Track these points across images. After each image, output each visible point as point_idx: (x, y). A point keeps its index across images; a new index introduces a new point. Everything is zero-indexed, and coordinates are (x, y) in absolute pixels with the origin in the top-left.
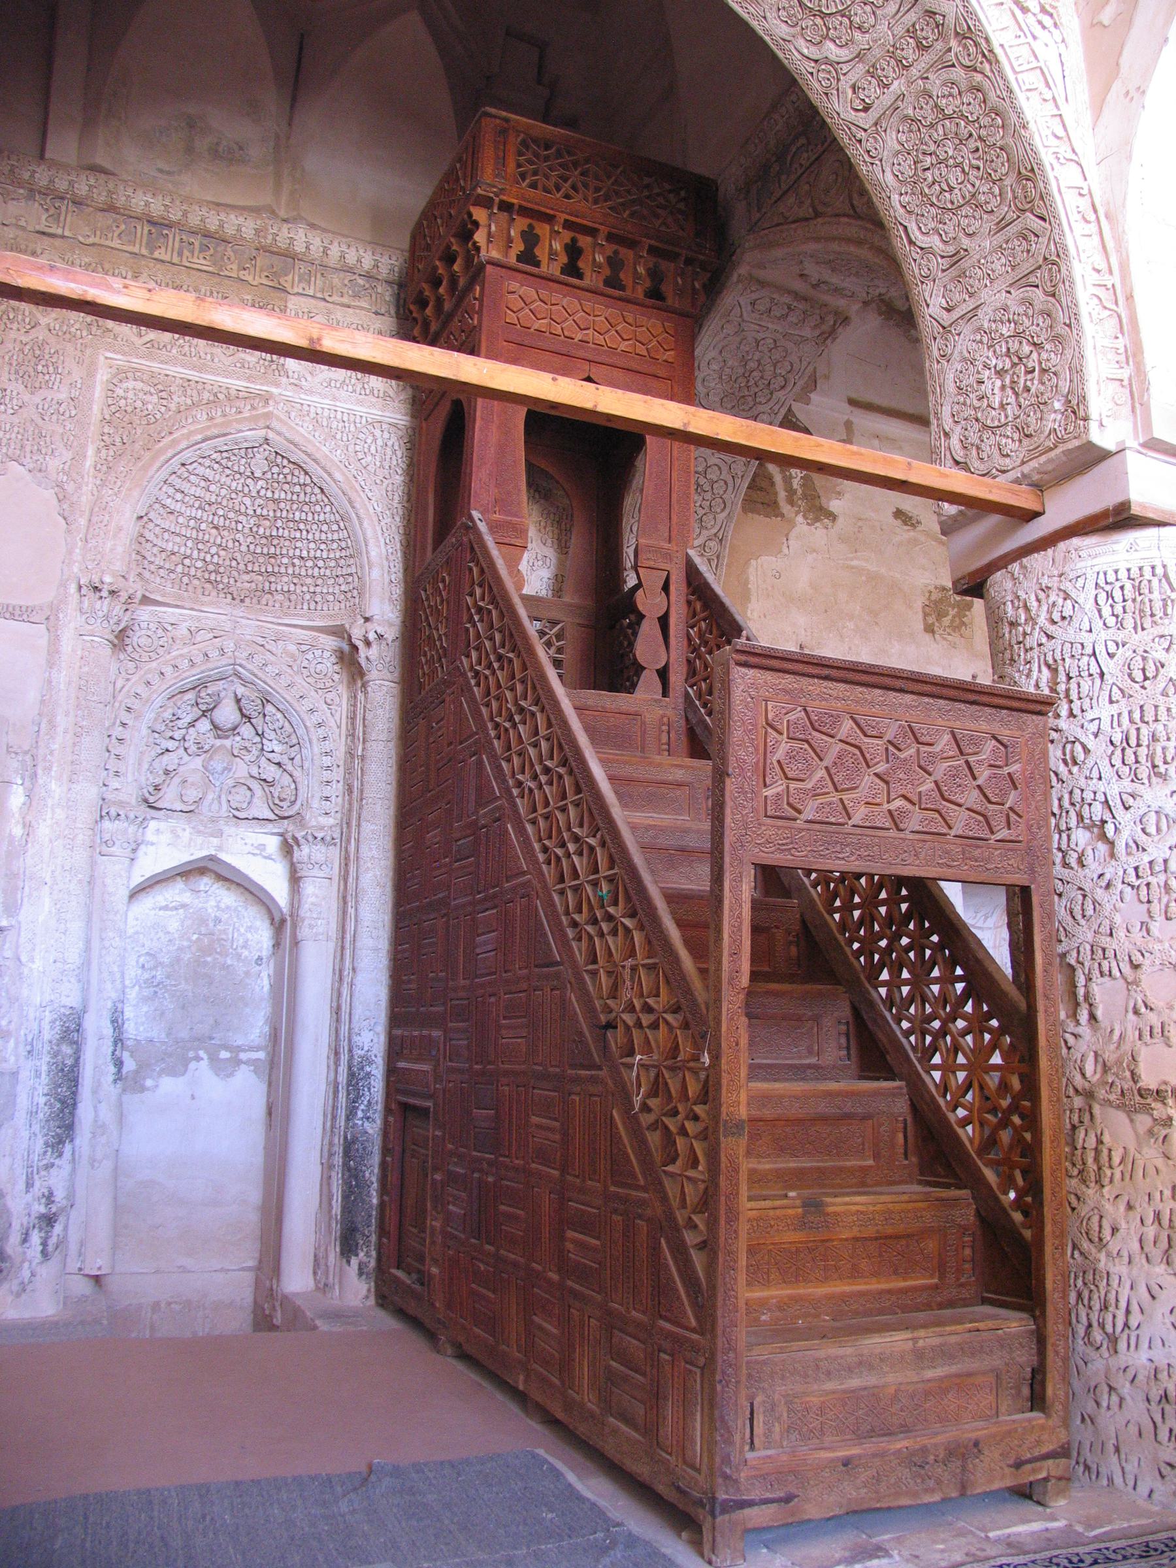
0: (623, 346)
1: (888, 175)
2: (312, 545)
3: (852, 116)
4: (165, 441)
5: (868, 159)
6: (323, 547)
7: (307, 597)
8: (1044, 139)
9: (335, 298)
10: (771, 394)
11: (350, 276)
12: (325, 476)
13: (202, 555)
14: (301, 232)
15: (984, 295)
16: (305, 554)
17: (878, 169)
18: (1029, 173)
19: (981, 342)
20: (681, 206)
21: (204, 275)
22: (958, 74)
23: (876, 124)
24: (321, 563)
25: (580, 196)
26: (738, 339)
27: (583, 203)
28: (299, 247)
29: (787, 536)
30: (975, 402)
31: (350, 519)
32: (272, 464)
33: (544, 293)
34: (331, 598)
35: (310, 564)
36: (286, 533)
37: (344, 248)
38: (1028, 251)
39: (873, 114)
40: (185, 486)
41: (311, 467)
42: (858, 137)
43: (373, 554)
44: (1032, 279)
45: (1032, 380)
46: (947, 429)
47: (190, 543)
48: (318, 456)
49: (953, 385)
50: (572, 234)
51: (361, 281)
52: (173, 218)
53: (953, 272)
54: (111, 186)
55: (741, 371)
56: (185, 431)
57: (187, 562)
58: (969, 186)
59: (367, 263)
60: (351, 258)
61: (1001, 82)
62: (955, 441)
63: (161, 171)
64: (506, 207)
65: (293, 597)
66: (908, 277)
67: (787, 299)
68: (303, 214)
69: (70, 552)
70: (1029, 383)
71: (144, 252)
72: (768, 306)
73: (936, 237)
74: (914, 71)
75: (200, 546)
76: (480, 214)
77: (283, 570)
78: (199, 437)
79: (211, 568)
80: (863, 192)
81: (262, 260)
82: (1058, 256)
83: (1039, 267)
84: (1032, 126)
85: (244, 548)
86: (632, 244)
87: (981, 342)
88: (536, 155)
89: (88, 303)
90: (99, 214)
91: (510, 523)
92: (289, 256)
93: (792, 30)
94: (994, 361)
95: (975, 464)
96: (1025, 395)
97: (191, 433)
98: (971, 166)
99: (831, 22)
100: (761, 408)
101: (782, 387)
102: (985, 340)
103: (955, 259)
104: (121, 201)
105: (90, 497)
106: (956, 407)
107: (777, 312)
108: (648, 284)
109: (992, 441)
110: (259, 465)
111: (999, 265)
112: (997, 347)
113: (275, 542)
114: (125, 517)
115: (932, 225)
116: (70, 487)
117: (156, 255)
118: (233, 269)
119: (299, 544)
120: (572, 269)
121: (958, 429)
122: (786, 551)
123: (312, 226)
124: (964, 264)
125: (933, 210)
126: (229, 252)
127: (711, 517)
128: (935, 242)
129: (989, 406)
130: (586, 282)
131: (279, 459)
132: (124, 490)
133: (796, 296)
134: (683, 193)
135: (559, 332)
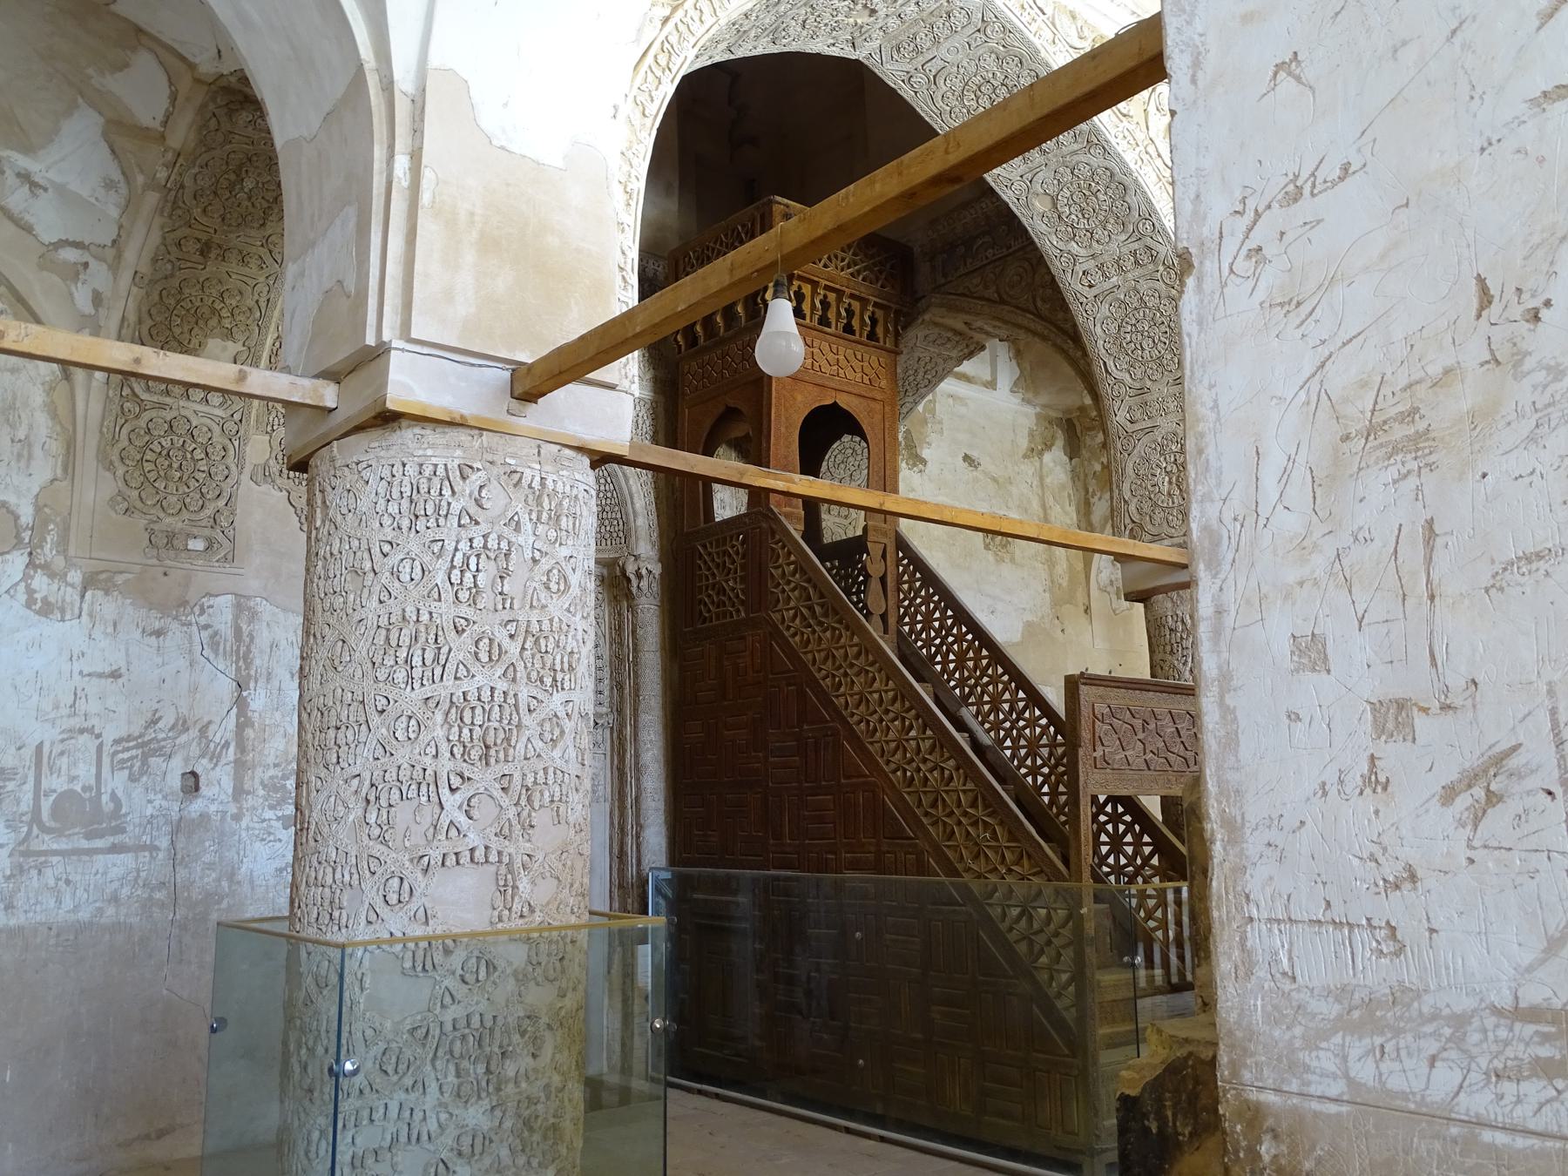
1: (1098, 330)
22: (1160, 285)
39: (1094, 291)
62: (1132, 508)
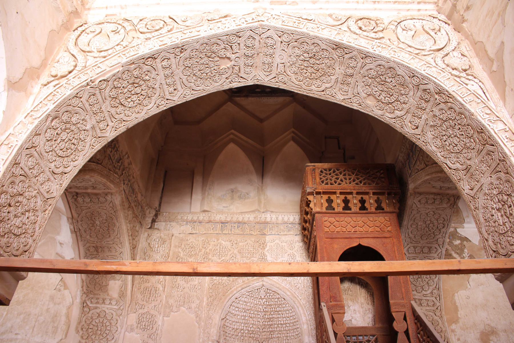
0: (370, 230)
2: (284, 319)
3: (413, 132)
4: (229, 292)
5: (424, 144)
6: (288, 319)
7: (285, 338)
8: (482, 116)
9: (282, 233)
10: (440, 230)
11: (286, 225)
12: (284, 294)
13: (247, 328)
14: (269, 215)
15: (483, 180)
16: (282, 322)
17: (429, 146)
18: (481, 130)
19: (487, 199)
20: (382, 175)
21: (239, 235)
22: (442, 106)
23: (422, 131)
24: (288, 325)
25: (344, 183)
26: (419, 215)
27: (346, 185)
28: (268, 220)
29: (468, 280)
30: (493, 224)
31: (295, 308)
32: (267, 293)
33: (337, 219)
34: (293, 337)
35: (284, 326)
36: (275, 316)
37: (283, 216)
38: (492, 159)
40: (238, 305)
41: (279, 292)
42: (418, 138)
43: (304, 319)
44: (498, 169)
45: (511, 210)
46: (486, 238)
47: (242, 325)
48: (281, 288)
49: (482, 219)
50: (344, 196)
51: (290, 226)
52: (228, 220)
53: (468, 175)
54: (209, 215)
55: (424, 225)
56: (235, 287)
57: (242, 331)
58: (462, 142)
59: (291, 219)
60: (286, 219)
61: (458, 103)
62: (490, 242)
63: (224, 207)
64: (318, 193)
65: (280, 339)
66: (454, 181)
67: (432, 196)
68: (268, 209)
69: (200, 335)
70: (511, 212)
71: (220, 232)
72: (426, 200)
73: (458, 164)
74: (427, 110)
75: (246, 325)
76: (310, 198)
77: (275, 329)
78: (240, 289)
79: (251, 332)
80: (428, 156)
81: (258, 226)
82: (504, 157)
83: (499, 164)
84: (475, 114)
85: (261, 324)
86: (367, 193)
87: (487, 199)
88: (326, 174)
89: (118, 271)
90: (207, 224)
91: (337, 305)
92: (266, 223)
93: (383, 111)
94: (495, 206)
95: (502, 251)
96: (511, 217)
97: (237, 288)
98: (460, 135)
99: (393, 104)
100: (437, 237)
101: (444, 227)
102: (489, 198)
103: (467, 170)
104: (212, 219)
105: (206, 315)
106: (487, 227)
107: (430, 202)
108: (376, 205)
109: (504, 240)
110: (262, 294)
111: (484, 168)
112: (494, 200)
113: (272, 320)
114: (217, 319)
115: (455, 160)
116: (199, 312)
117: (224, 232)
118: (247, 231)
119: (280, 319)
120: (347, 207)
121: (490, 237)
122: (469, 287)
123: (272, 212)
124: (471, 171)
125: (453, 155)
126: (247, 226)
127: (432, 281)
128: (458, 165)
129: (499, 225)
130: (353, 210)
131: (269, 291)
132: (216, 311)
133: (435, 194)
134: (382, 171)
135: (345, 230)
